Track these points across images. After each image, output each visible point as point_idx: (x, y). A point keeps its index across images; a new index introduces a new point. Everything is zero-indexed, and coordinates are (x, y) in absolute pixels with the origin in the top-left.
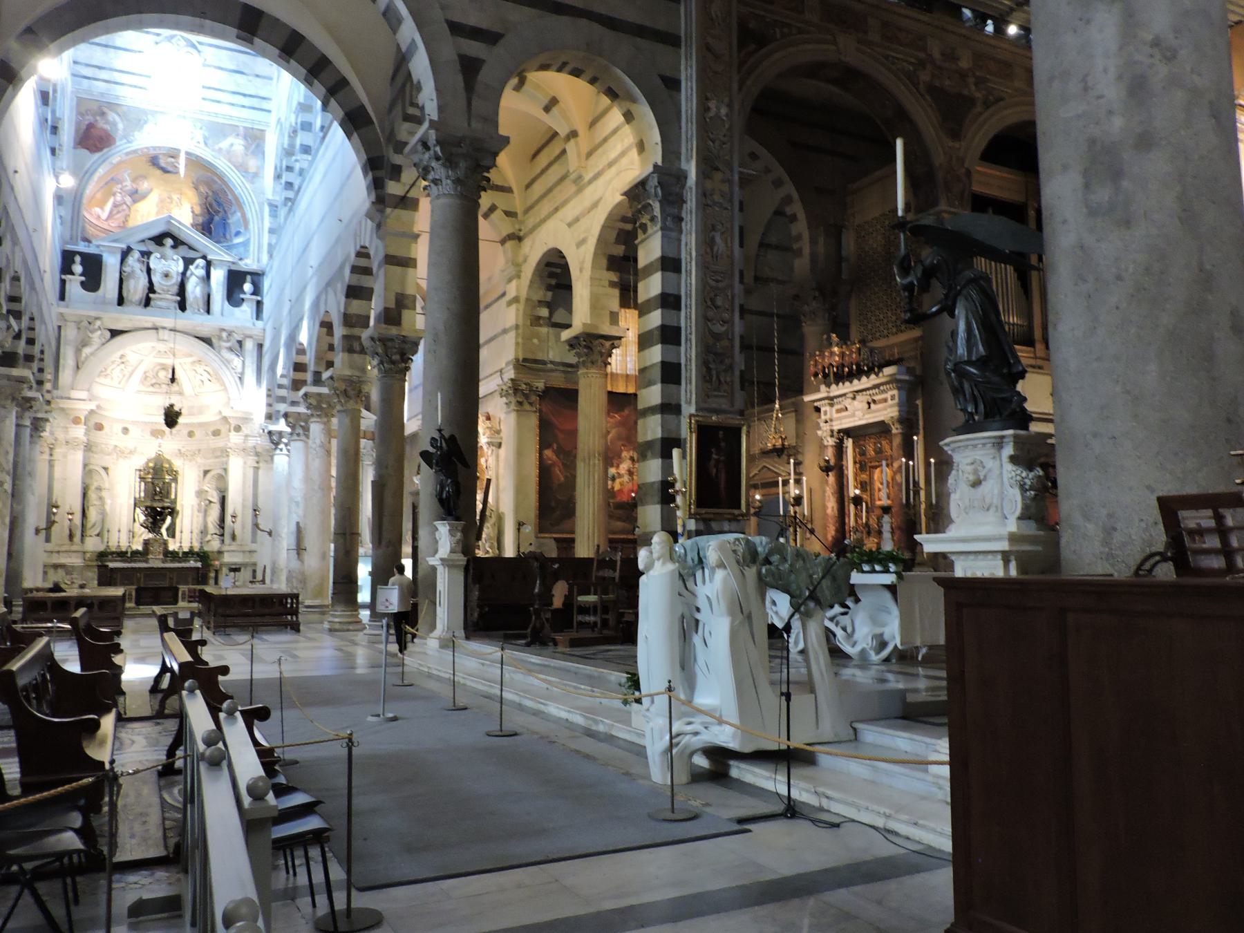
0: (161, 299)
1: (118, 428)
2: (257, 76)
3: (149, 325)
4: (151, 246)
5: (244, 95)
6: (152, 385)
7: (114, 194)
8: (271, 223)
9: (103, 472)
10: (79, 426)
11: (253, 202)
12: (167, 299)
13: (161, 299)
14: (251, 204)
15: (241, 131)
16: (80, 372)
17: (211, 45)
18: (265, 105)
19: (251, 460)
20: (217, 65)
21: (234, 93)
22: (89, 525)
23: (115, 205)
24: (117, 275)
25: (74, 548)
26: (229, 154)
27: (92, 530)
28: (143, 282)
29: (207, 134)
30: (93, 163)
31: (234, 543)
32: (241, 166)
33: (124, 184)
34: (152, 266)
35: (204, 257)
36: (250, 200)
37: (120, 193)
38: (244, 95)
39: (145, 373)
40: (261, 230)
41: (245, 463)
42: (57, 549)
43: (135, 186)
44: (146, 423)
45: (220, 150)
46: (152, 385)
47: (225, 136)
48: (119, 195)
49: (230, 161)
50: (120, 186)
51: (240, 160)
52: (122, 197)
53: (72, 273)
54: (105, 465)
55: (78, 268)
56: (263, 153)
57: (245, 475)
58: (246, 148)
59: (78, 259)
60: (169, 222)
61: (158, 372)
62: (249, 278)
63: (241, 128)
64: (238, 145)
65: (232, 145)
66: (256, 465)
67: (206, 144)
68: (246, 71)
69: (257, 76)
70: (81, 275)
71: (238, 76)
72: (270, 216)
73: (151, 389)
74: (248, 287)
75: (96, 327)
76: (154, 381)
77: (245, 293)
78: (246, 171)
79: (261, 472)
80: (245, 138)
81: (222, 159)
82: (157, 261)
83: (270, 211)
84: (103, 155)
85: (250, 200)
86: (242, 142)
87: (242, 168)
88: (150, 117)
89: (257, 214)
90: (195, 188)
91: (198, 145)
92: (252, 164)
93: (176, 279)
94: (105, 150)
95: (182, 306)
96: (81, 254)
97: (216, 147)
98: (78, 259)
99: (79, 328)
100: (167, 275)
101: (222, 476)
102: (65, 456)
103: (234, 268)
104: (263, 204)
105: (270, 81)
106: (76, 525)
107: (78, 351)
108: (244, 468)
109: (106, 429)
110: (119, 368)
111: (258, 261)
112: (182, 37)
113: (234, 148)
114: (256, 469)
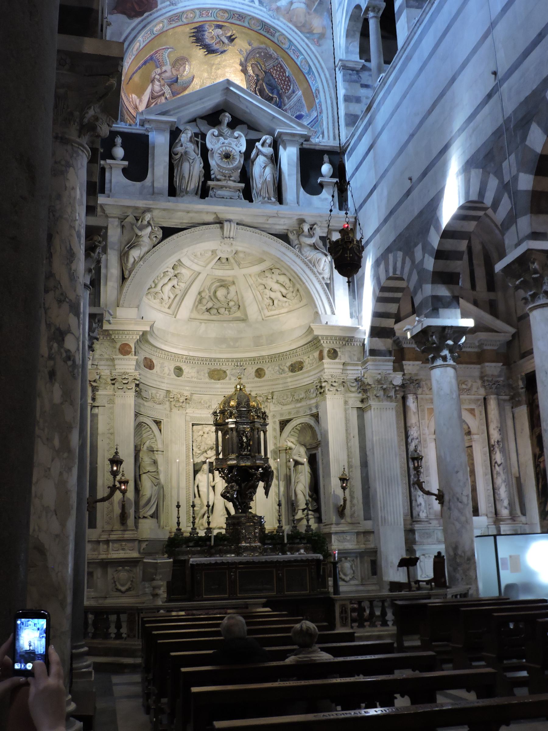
0: (222, 187)
1: (170, 367)
3: (210, 218)
4: (203, 126)
6: (208, 310)
7: (153, 81)
8: (346, 89)
9: (154, 427)
10: (130, 356)
11: (322, 68)
12: (230, 188)
13: (222, 187)
14: (320, 71)
16: (128, 283)
19: (354, 399)
22: (143, 502)
23: (153, 97)
24: (167, 159)
25: (128, 535)
27: (147, 508)
28: (198, 166)
30: (133, 29)
31: (343, 521)
32: (304, 26)
33: (164, 69)
34: (209, 145)
35: (271, 133)
36: (318, 65)
37: (159, 81)
39: (200, 293)
41: (346, 403)
42: (104, 537)
43: (175, 73)
44: (203, 360)
45: (278, 9)
46: (208, 310)
48: (157, 83)
49: (290, 21)
50: (158, 71)
51: (302, 19)
52: (161, 86)
53: (113, 158)
54: (158, 417)
55: (119, 152)
57: (347, 420)
59: (119, 140)
60: (228, 89)
61: (215, 292)
62: (326, 158)
66: (360, 405)
70: (123, 159)
72: (344, 81)
73: (206, 316)
74: (326, 168)
75: (145, 223)
76: (210, 305)
77: (322, 176)
79: (369, 416)
81: (281, 19)
82: (214, 140)
83: (344, 75)
84: (142, 21)
85: (318, 65)
89: (327, 81)
90: (242, 71)
93: (239, 161)
94: (146, 14)
95: (248, 195)
96: (123, 135)
97: (274, 6)
98: (119, 140)
99: (123, 227)
100: (227, 156)
101: (311, 427)
102: (111, 401)
103: (306, 146)
106: (129, 499)
107: (123, 256)
108: (346, 410)
109: (157, 369)
110: (170, 285)
113: (294, 6)
114: (361, 411)
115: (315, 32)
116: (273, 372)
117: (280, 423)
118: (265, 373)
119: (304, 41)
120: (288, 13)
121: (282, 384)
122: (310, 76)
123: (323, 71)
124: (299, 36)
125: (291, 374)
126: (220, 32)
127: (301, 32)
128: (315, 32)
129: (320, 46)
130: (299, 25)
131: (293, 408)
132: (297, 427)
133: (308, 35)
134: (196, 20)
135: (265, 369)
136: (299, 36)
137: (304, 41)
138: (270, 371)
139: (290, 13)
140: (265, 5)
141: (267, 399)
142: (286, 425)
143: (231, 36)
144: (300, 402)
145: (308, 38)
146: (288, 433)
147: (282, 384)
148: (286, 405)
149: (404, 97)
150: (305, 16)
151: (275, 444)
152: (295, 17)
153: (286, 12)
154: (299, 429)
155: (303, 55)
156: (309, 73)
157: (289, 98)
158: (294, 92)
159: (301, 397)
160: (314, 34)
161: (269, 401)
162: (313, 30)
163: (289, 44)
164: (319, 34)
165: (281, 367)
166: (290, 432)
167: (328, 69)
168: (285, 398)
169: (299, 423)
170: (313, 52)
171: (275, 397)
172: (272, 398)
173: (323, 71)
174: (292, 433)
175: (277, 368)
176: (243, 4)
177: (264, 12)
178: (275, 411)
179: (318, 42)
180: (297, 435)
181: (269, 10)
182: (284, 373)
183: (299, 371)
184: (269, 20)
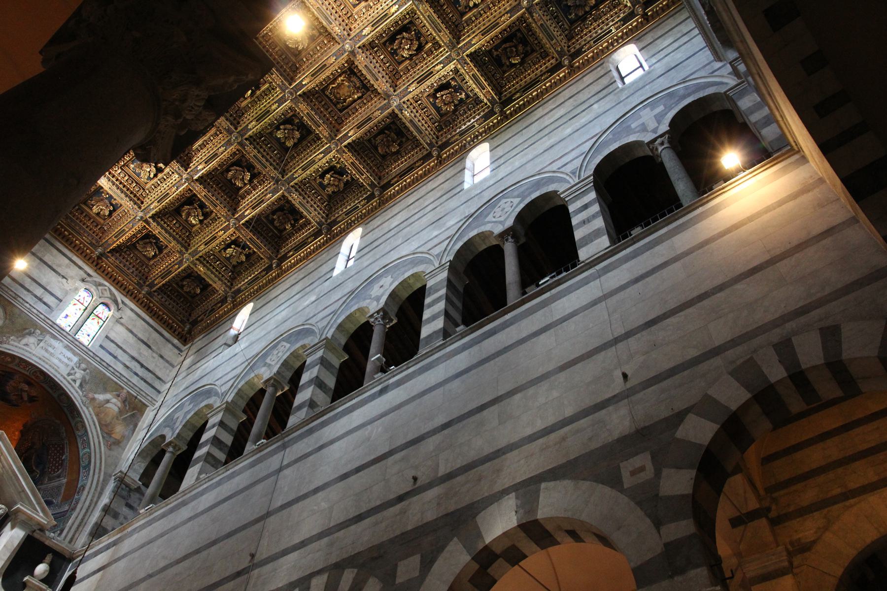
2: (161, 357)
5: (142, 366)
11: (100, 469)
14: (97, 471)
15: (124, 394)
17: (132, 310)
18: (157, 384)
20: (130, 327)
21: (133, 358)
26: (100, 409)
29: (87, 378)
32: (106, 426)
36: (98, 465)
38: (142, 366)
40: (94, 504)
45: (93, 399)
47: (105, 390)
49: (97, 415)
51: (108, 420)
56: (136, 426)
58: (121, 412)
62: (49, 558)
63: (125, 391)
64: (114, 405)
65: (108, 401)
67: (81, 386)
68: (153, 347)
69: (161, 357)
71: (144, 347)
74: (41, 569)
78: (109, 434)
80: (124, 402)
81: (90, 409)
85: (98, 465)
86: (119, 404)
87: (106, 429)
88: (38, 331)
89: (97, 483)
91: (73, 383)
92: (119, 430)
97: (90, 395)
103: (37, 535)
104: (110, 476)
105: (171, 368)
111: (70, 542)
112: (109, 289)
113: (108, 405)
115: (113, 436)
119: (98, 438)
120: (99, 407)
122: (84, 471)
123: (100, 473)
124: (97, 431)
126: (26, 387)
127: (101, 429)
128: (113, 436)
129: (110, 449)
130: (103, 422)
133: (105, 435)
134: (10, 366)
136: (97, 431)
137: (98, 438)
139: (101, 408)
140: (83, 389)
143: (33, 397)
145: (103, 437)
149: (162, 535)
150: (113, 418)
152: (103, 414)
153: (98, 406)
155: (90, 449)
156: (85, 468)
157: (50, 479)
158: (59, 476)
160: (111, 437)
162: (113, 434)
163: (83, 432)
164: (116, 439)
167: (104, 473)
170: (101, 452)
173: (100, 473)
176: (64, 378)
177: (79, 395)
179: (110, 445)
181: (85, 396)
184: (79, 404)
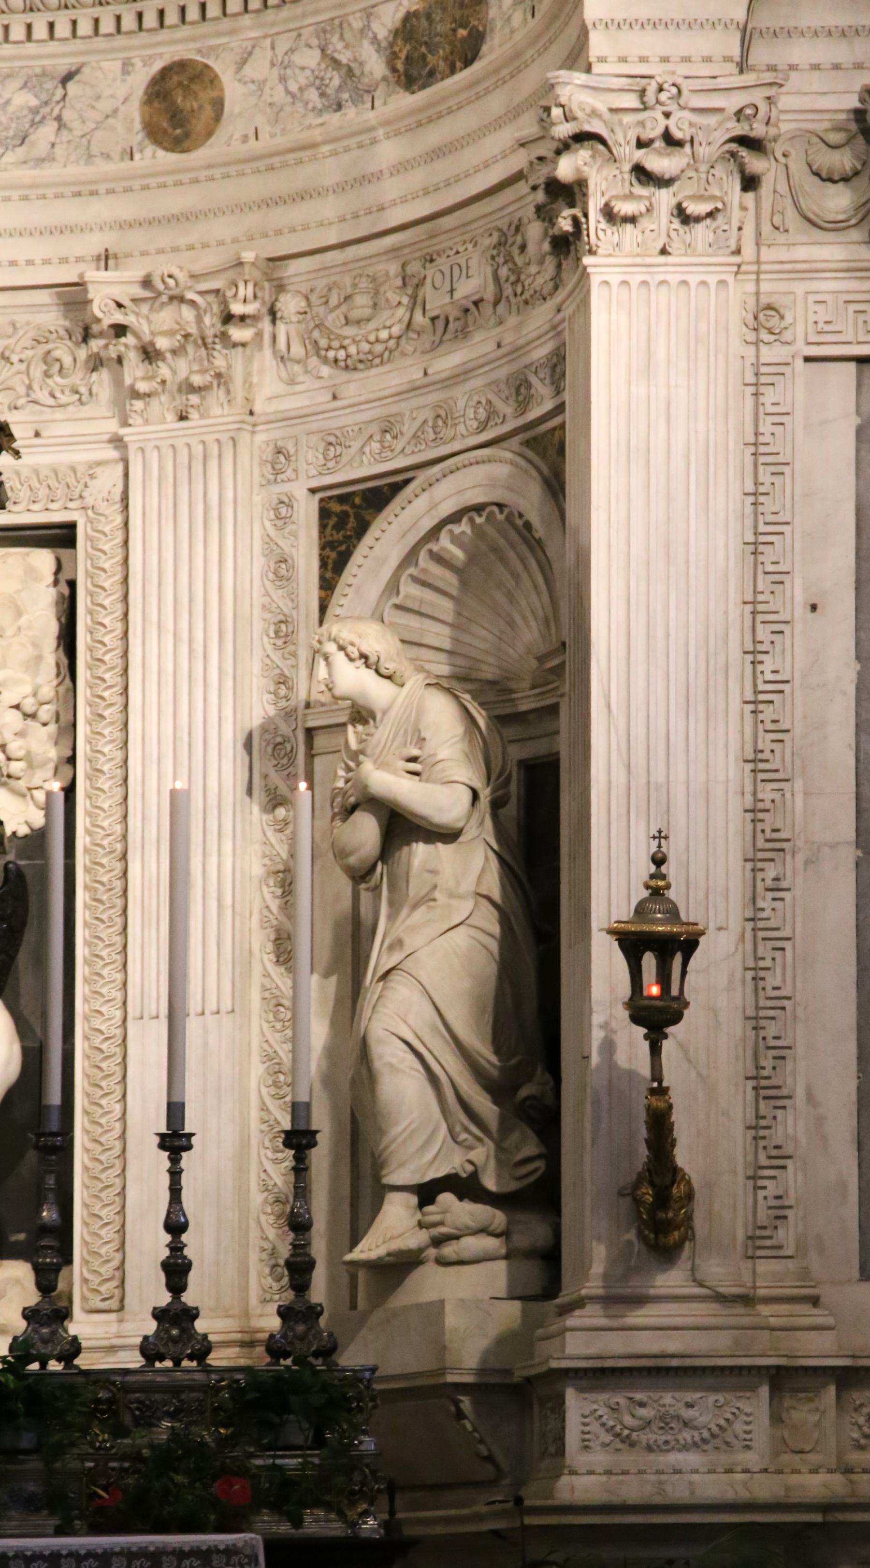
116: (279, 95)
117: (324, 514)
118: (218, 105)
121: (340, 188)
125: (405, 101)
131: (414, 389)
132: (444, 542)
135: (224, 68)
138: (261, 85)
141: (228, 318)
142: (362, 529)
144: (463, 334)
146: (374, 591)
147: (340, 188)
148: (366, 362)
151: (283, 680)
154: (459, 554)
159: (466, 289)
161: (237, 333)
165: (336, 44)
166: (393, 587)
168: (362, 300)
169: (447, 508)
171: (290, 305)
172: (273, 313)
174: (409, 590)
175: (310, 58)
178: (286, 418)
180: (445, 607)
182: (357, 99)
183: (453, 71)
